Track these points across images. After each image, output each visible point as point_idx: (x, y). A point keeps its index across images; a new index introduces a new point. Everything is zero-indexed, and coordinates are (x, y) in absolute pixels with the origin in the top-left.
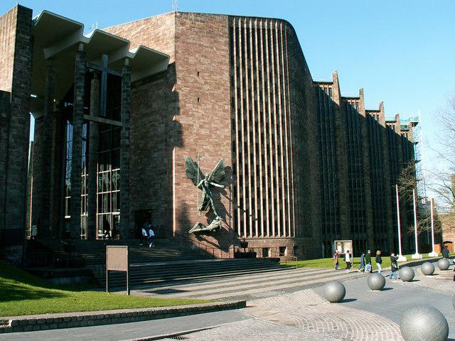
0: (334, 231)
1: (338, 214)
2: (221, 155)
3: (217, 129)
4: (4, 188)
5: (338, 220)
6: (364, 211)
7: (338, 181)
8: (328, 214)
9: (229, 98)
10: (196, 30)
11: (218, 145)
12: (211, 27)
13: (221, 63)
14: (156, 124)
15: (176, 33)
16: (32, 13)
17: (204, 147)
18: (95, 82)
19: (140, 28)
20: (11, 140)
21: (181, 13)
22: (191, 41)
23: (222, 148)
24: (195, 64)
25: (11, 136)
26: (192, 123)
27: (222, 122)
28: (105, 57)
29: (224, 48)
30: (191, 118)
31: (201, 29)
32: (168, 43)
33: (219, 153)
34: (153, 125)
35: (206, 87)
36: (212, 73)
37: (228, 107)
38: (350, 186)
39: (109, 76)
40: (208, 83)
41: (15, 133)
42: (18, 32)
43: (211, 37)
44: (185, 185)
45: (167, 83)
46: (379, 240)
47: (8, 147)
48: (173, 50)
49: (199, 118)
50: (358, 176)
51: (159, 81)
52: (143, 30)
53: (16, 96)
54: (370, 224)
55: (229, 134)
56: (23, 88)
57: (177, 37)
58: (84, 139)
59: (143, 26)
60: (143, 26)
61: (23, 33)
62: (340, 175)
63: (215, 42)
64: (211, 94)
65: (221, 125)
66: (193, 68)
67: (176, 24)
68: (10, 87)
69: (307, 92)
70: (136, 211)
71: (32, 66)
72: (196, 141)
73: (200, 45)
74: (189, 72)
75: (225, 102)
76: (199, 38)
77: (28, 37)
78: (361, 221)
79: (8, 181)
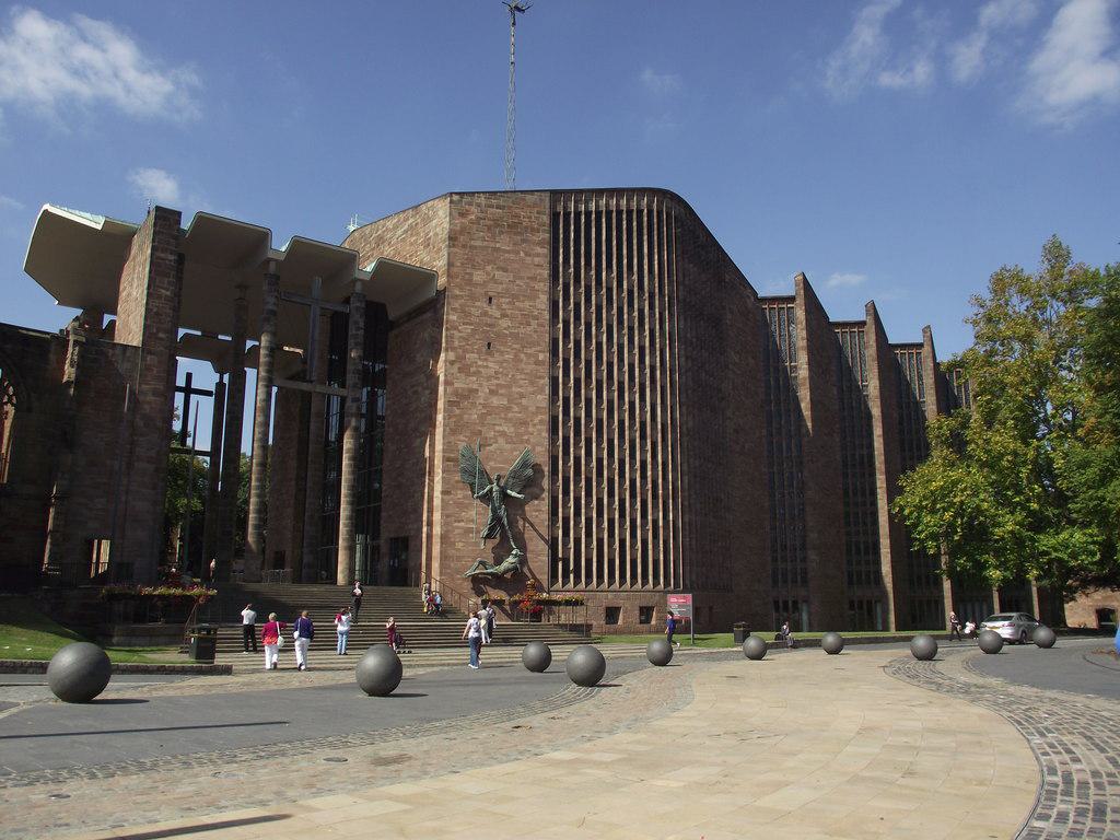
1: (804, 547)
2: (528, 441)
3: (522, 396)
5: (804, 560)
8: (784, 547)
9: (547, 340)
11: (525, 423)
12: (518, 216)
13: (533, 278)
14: (420, 389)
15: (451, 230)
16: (180, 217)
17: (497, 428)
21: (461, 194)
22: (478, 243)
23: (530, 429)
27: (532, 383)
29: (539, 250)
30: (475, 379)
31: (497, 223)
32: (440, 249)
33: (526, 437)
34: (416, 392)
35: (505, 323)
36: (515, 297)
37: (544, 356)
40: (507, 316)
42: (154, 249)
43: (515, 234)
44: (460, 494)
49: (489, 378)
52: (411, 227)
53: (150, 353)
55: (545, 404)
56: (161, 339)
57: (452, 238)
62: (806, 473)
63: (523, 241)
65: (531, 389)
70: (391, 539)
72: (482, 417)
73: (496, 250)
74: (473, 298)
75: (539, 348)
76: (494, 237)
77: (172, 258)
78: (867, 563)
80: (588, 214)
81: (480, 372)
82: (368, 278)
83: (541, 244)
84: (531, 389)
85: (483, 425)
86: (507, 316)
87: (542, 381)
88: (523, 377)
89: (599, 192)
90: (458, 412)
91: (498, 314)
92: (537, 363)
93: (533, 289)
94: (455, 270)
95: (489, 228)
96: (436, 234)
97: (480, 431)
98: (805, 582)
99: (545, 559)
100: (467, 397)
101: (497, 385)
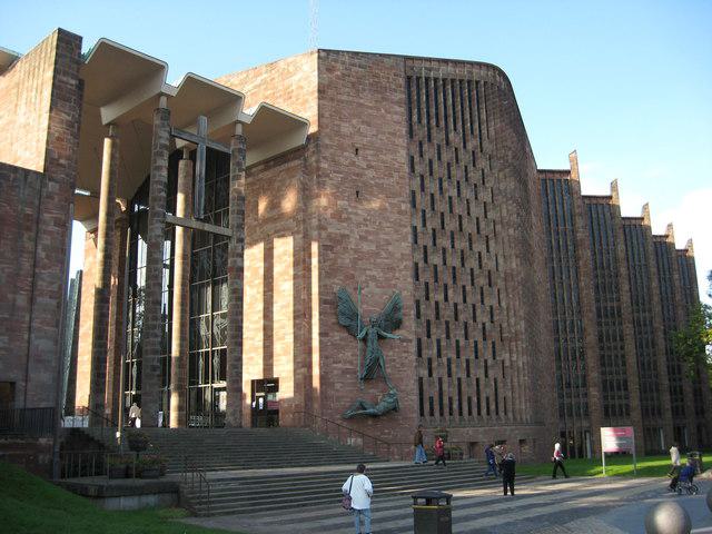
0: (579, 415)
1: (584, 385)
2: (395, 286)
4: (26, 336)
6: (626, 381)
7: (582, 330)
8: (569, 385)
10: (353, 80)
11: (391, 269)
13: (394, 134)
18: (186, 165)
19: (259, 79)
20: (42, 254)
21: (328, 52)
22: (344, 98)
24: (351, 136)
25: (40, 247)
26: (347, 232)
27: (397, 231)
28: (203, 120)
29: (398, 109)
32: (306, 101)
33: (393, 282)
35: (370, 173)
36: (379, 150)
37: (406, 207)
38: (601, 340)
39: (209, 150)
40: (372, 167)
41: (48, 242)
42: (56, 71)
45: (305, 167)
46: (648, 429)
47: (35, 266)
48: (316, 112)
50: (614, 324)
51: (292, 164)
52: (264, 82)
53: (51, 179)
54: (635, 402)
55: (408, 251)
56: (61, 165)
58: (165, 266)
59: (265, 76)
60: (265, 76)
61: (65, 74)
62: (585, 321)
64: (377, 185)
65: (395, 237)
66: (347, 142)
67: (319, 68)
68: (42, 163)
69: (530, 186)
71: (79, 128)
72: (355, 261)
73: (361, 105)
74: (341, 148)
75: (401, 199)
77: (73, 82)
79: (34, 324)
80: (436, 80)
81: (350, 219)
82: (248, 121)
83: (399, 103)
84: (395, 237)
85: (355, 269)
86: (372, 167)
87: (405, 230)
88: (388, 225)
89: (446, 61)
90: (332, 256)
91: (364, 165)
92: (400, 212)
93: (394, 144)
94: (324, 120)
95: (353, 84)
96: (302, 88)
97: (353, 277)
98: (587, 414)
99: (416, 398)
100: (339, 242)
101: (367, 232)
